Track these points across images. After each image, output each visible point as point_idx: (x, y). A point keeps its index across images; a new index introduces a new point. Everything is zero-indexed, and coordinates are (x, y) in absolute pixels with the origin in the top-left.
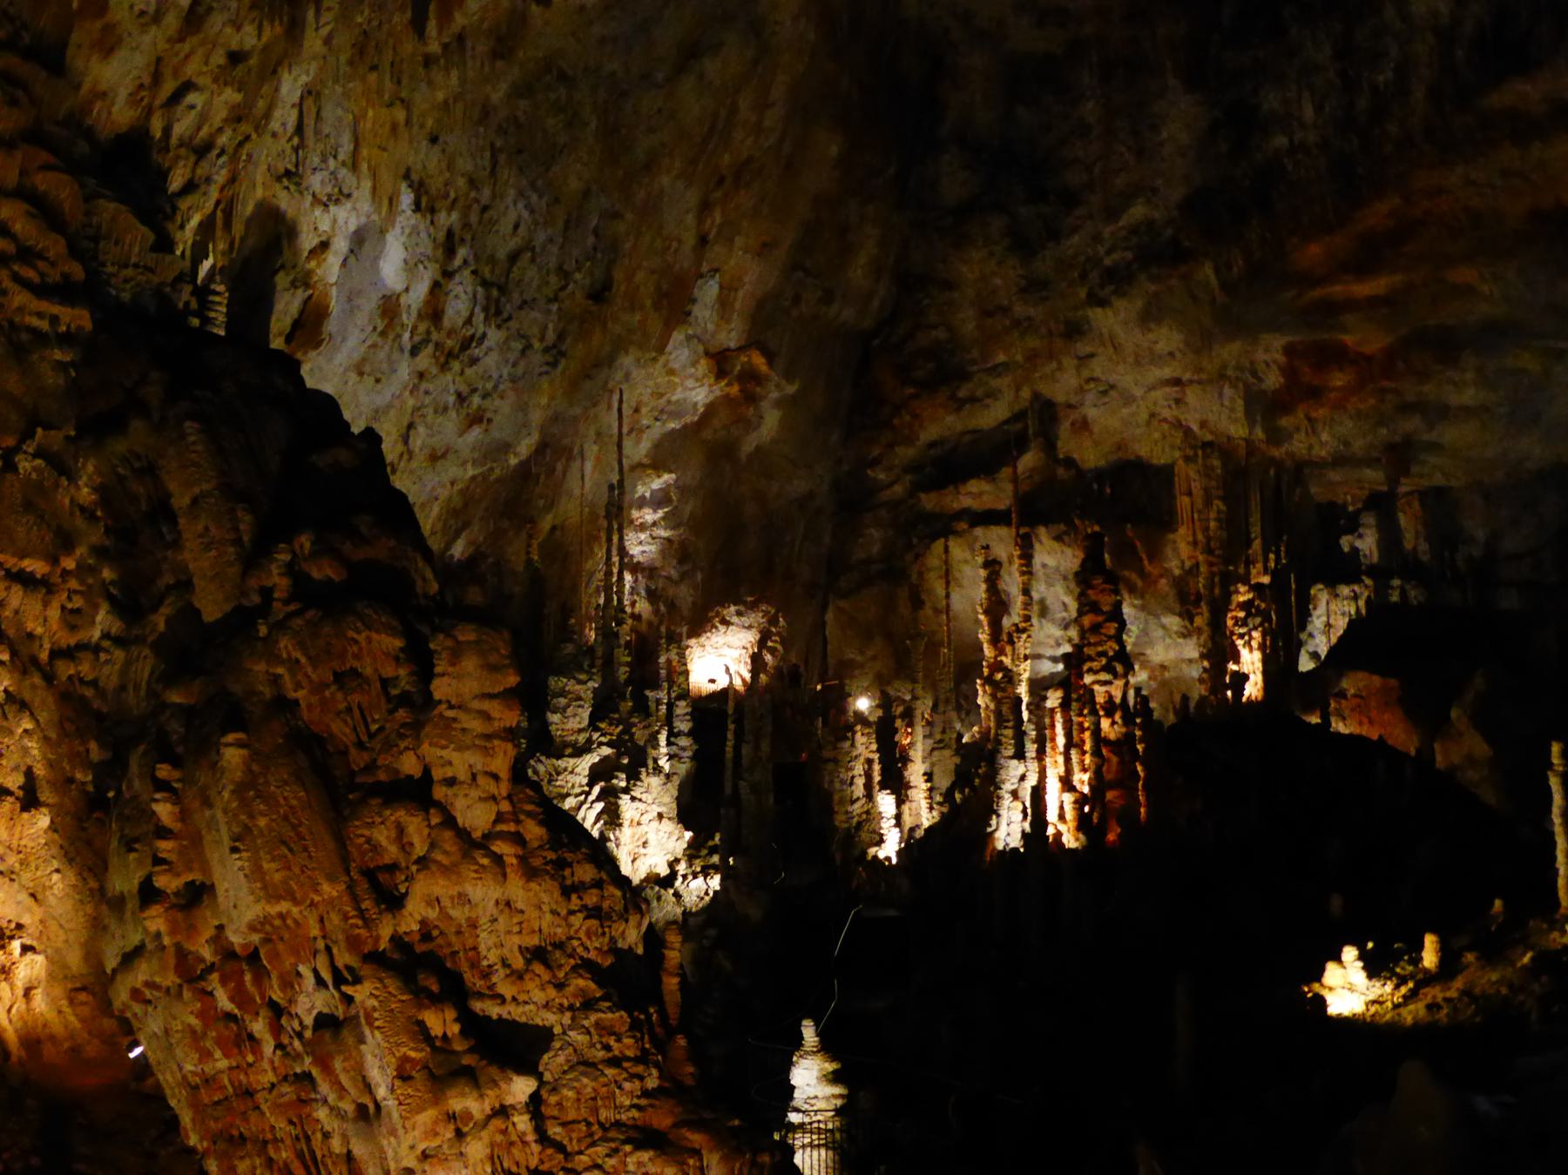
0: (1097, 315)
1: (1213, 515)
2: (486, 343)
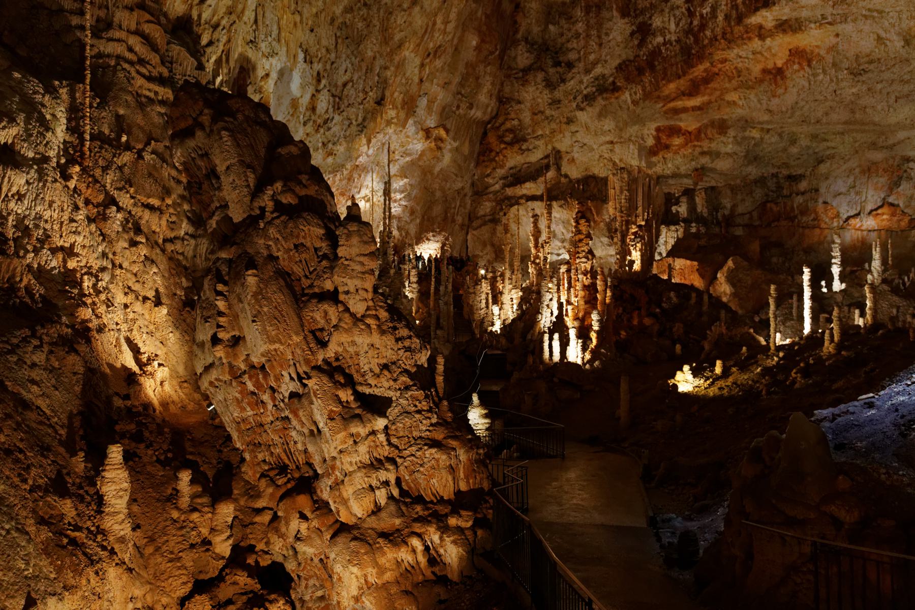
0: (579, 114)
2: (334, 121)
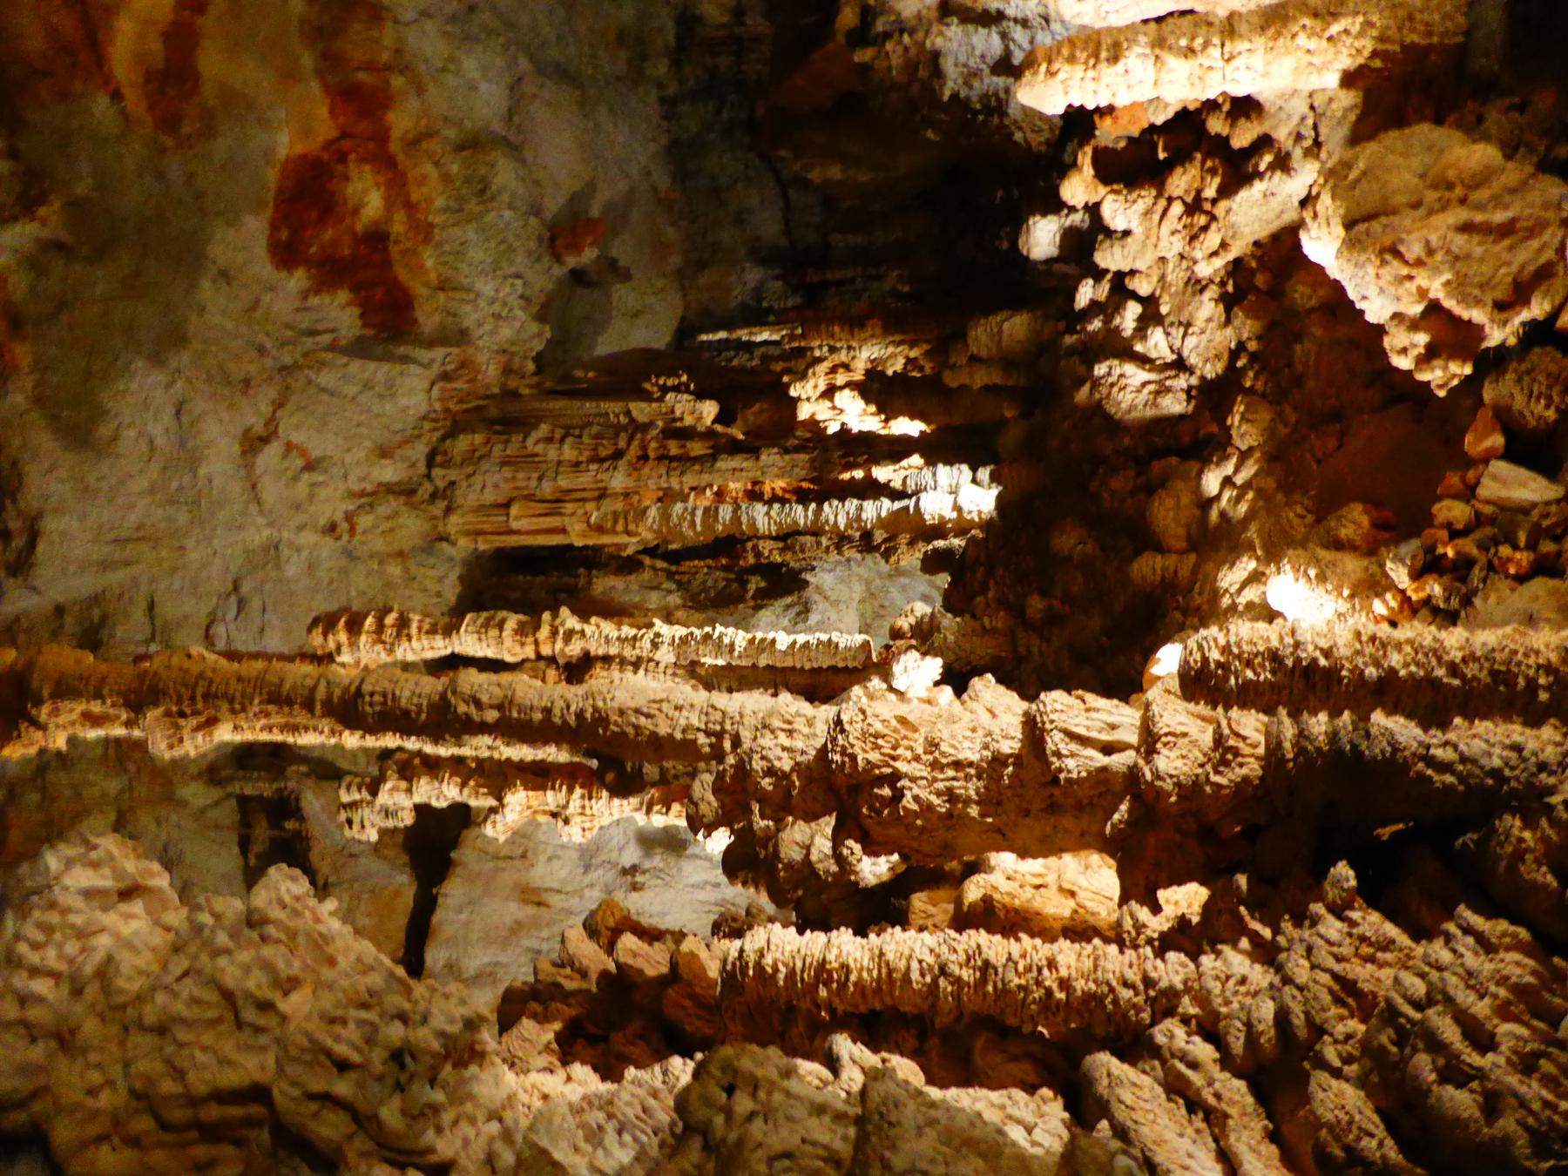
1: (552, 454)
